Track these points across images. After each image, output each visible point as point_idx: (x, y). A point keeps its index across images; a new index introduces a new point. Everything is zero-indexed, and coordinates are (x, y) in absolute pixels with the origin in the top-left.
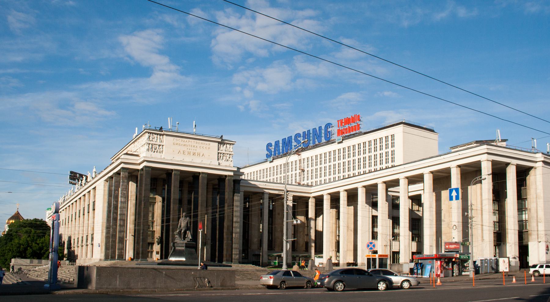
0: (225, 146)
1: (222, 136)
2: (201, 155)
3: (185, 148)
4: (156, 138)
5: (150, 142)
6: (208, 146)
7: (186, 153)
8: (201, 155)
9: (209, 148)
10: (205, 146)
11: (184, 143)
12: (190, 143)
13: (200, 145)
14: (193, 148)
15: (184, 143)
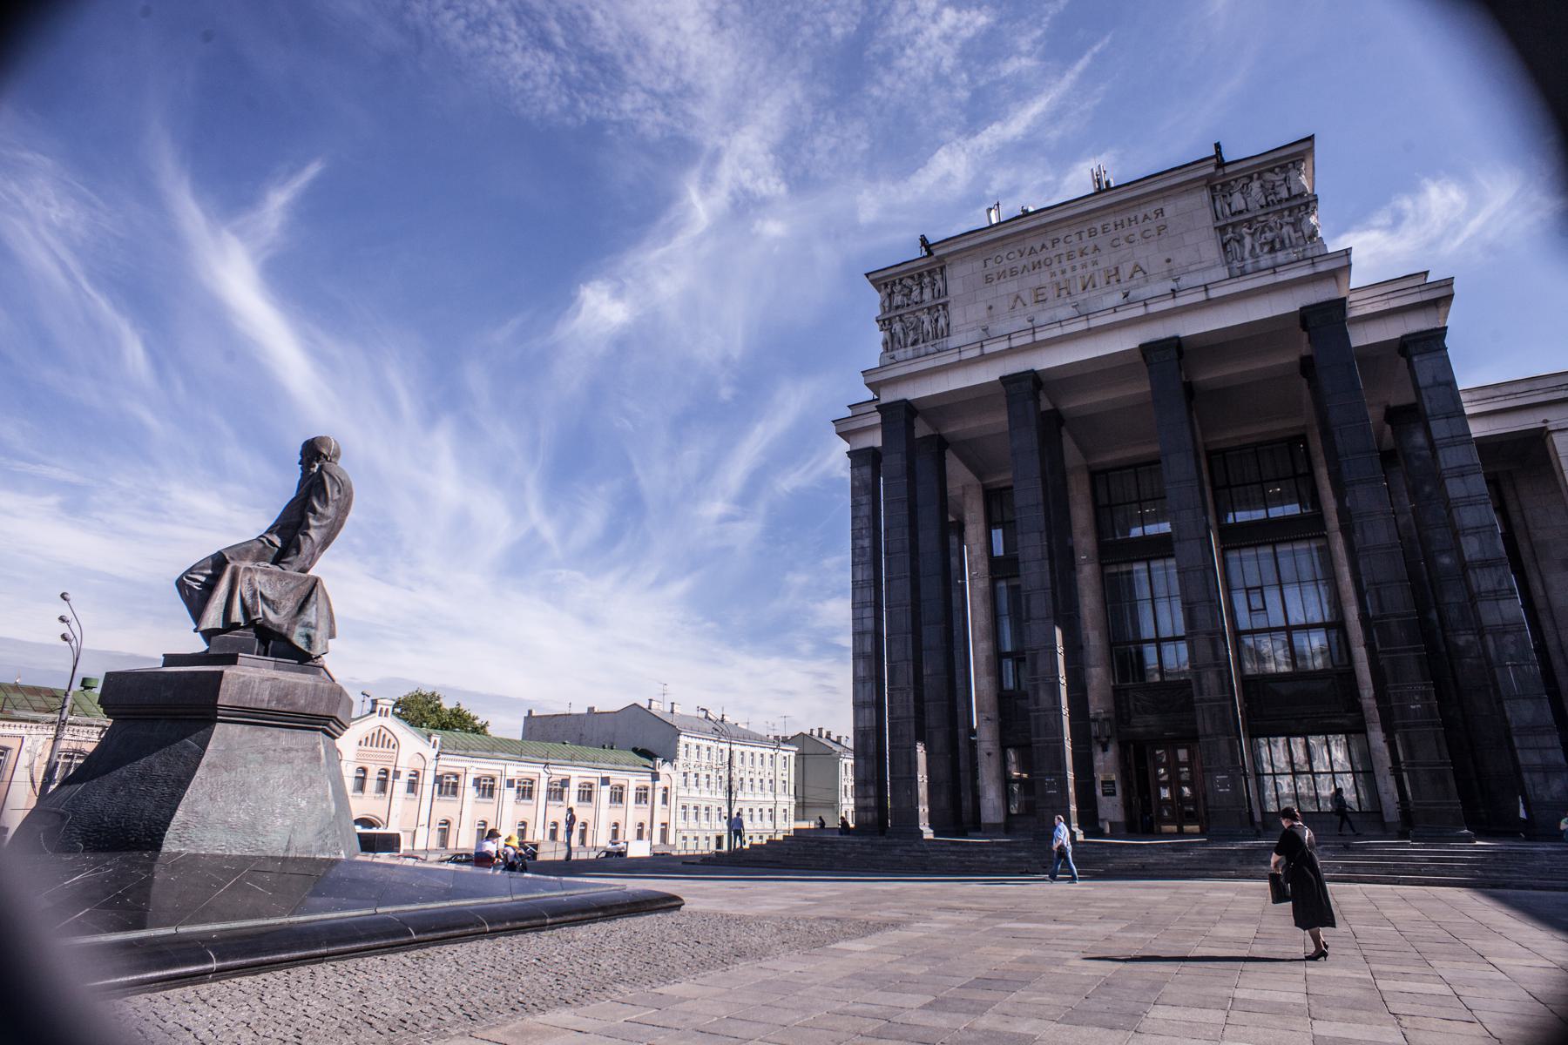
0: (1256, 185)
1: (1218, 146)
2: (1126, 270)
3: (1044, 278)
4: (916, 292)
5: (892, 314)
6: (1152, 225)
7: (1050, 293)
8: (1126, 270)
9: (1161, 229)
10: (1136, 230)
11: (1035, 258)
12: (1062, 248)
13: (1113, 234)
14: (1078, 261)
15: (1035, 258)
